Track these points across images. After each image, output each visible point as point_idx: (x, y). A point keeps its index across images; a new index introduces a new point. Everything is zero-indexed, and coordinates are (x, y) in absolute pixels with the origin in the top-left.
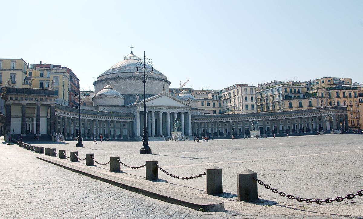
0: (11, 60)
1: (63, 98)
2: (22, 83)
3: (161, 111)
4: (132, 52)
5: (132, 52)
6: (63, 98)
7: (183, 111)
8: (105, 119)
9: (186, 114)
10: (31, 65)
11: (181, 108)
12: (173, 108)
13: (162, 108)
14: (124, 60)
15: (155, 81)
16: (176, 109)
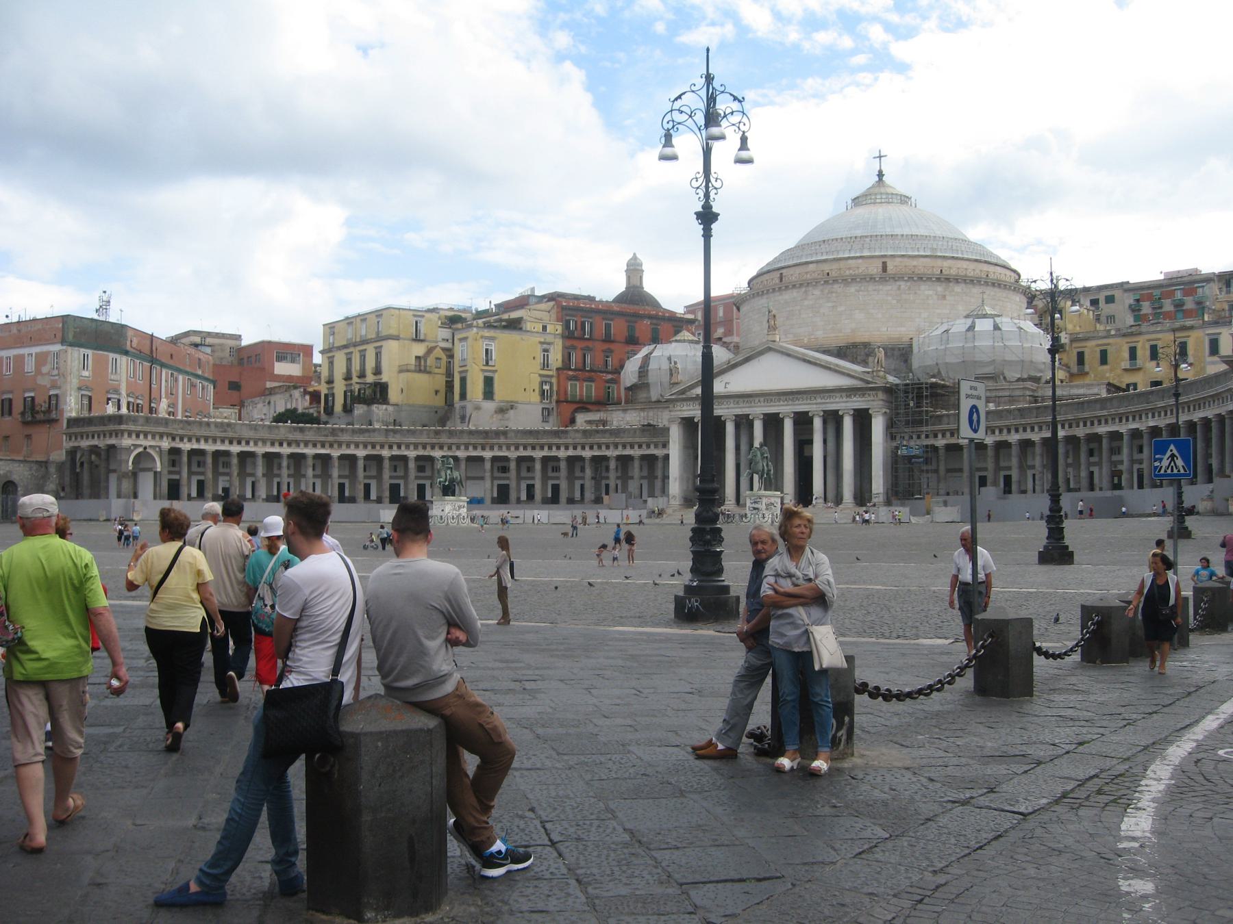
0: (377, 314)
1: (489, 394)
2: (396, 369)
3: (757, 411)
4: (881, 174)
5: (881, 174)
6: (489, 394)
7: (846, 406)
8: (571, 452)
9: (862, 420)
10: (495, 305)
11: (838, 395)
12: (805, 396)
13: (762, 399)
14: (849, 208)
15: (852, 289)
16: (819, 401)
